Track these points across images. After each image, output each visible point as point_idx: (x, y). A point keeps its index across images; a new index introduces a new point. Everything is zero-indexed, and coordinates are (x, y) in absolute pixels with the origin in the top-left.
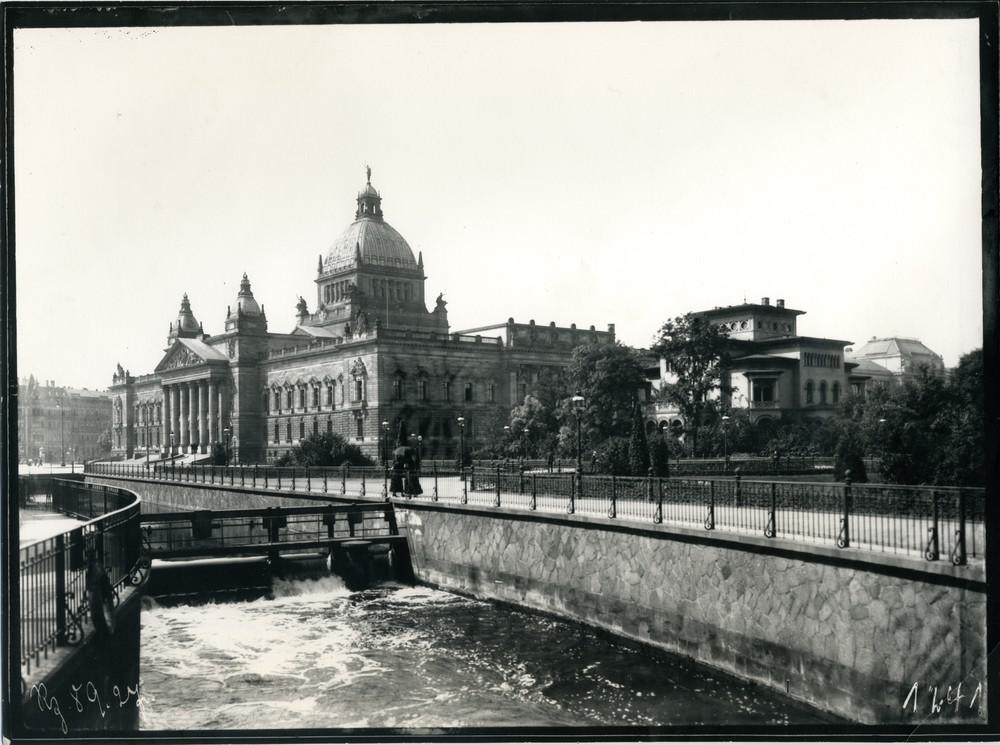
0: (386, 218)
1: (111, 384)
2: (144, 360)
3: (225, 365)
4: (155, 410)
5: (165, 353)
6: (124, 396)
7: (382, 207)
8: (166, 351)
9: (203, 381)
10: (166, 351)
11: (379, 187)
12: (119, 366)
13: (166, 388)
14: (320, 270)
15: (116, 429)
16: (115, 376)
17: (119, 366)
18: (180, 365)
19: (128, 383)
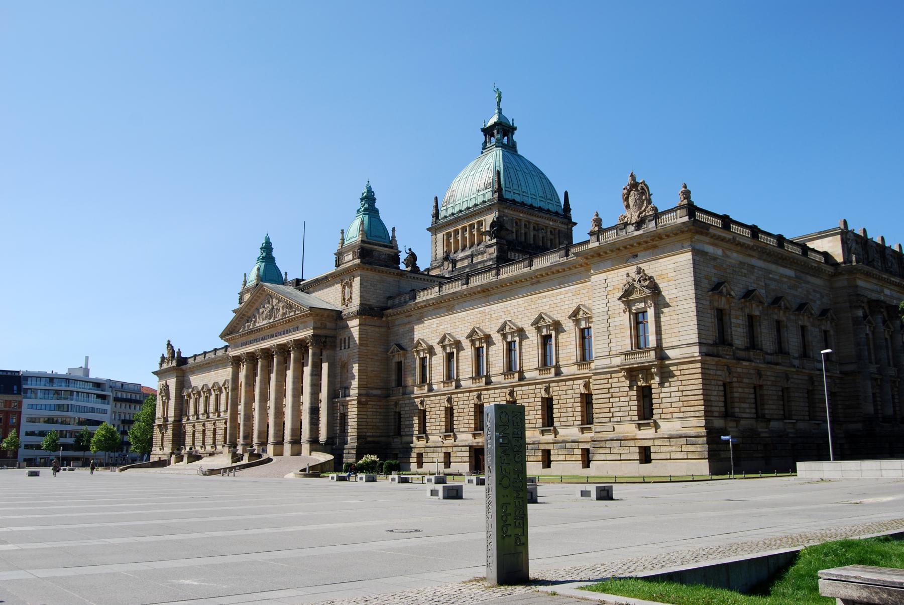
0: (521, 151)
1: (157, 368)
2: (201, 336)
3: (337, 316)
4: (212, 399)
5: (234, 314)
6: (172, 383)
7: (515, 138)
8: (234, 311)
9: (301, 345)
10: (234, 311)
11: (509, 115)
12: (169, 344)
13: (237, 362)
14: (436, 215)
15: (159, 426)
16: (163, 358)
17: (169, 344)
18: (261, 322)
19: (178, 365)
